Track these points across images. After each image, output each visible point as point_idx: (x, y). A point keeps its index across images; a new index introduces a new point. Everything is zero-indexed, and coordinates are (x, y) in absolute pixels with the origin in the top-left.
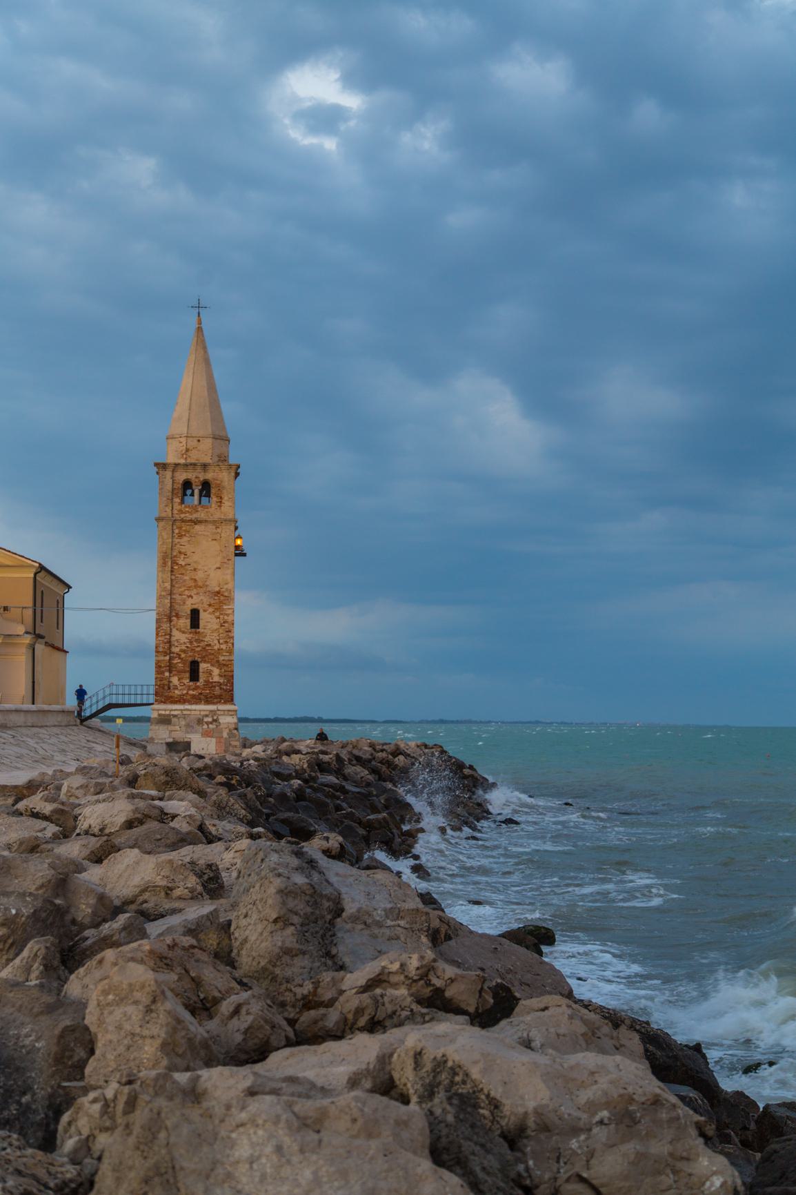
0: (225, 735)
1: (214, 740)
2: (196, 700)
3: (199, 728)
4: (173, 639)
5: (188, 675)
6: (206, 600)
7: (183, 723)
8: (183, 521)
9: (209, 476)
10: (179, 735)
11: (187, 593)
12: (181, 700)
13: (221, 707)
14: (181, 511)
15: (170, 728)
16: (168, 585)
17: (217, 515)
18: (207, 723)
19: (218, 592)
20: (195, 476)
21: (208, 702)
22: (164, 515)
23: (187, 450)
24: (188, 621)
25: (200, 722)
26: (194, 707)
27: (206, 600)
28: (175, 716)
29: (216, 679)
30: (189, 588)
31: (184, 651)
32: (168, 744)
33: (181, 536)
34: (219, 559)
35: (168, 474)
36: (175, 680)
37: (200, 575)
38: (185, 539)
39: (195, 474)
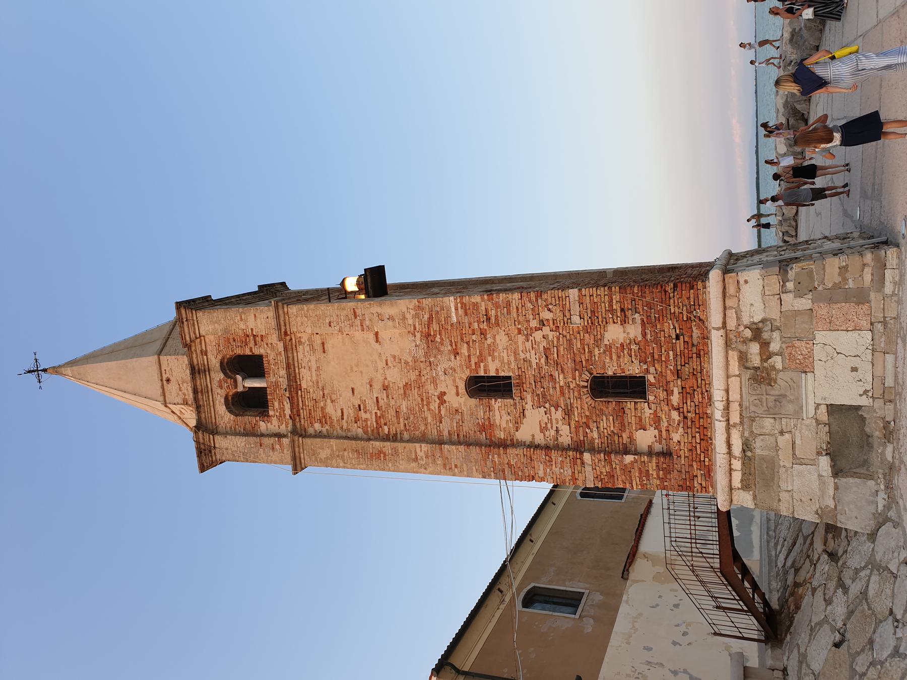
0: (804, 303)
1: (821, 336)
2: (696, 386)
3: (783, 379)
4: (540, 439)
5: (629, 405)
6: (445, 362)
7: (768, 423)
8: (295, 415)
9: (215, 362)
10: (808, 436)
11: (434, 405)
12: (698, 423)
13: (715, 319)
14: (280, 417)
15: (785, 459)
16: (422, 449)
17: (273, 338)
18: (766, 354)
19: (428, 336)
20: (219, 390)
21: (701, 352)
22: (288, 453)
23: (185, 403)
24: (497, 404)
25: (761, 377)
26: (718, 395)
27: (445, 362)
28: (747, 446)
29: (634, 331)
30: (425, 401)
31: (568, 413)
32: (837, 472)
33: (324, 419)
34: (358, 335)
35: (220, 441)
36: (645, 438)
37: (395, 376)
38: (330, 409)
39: (217, 390)
